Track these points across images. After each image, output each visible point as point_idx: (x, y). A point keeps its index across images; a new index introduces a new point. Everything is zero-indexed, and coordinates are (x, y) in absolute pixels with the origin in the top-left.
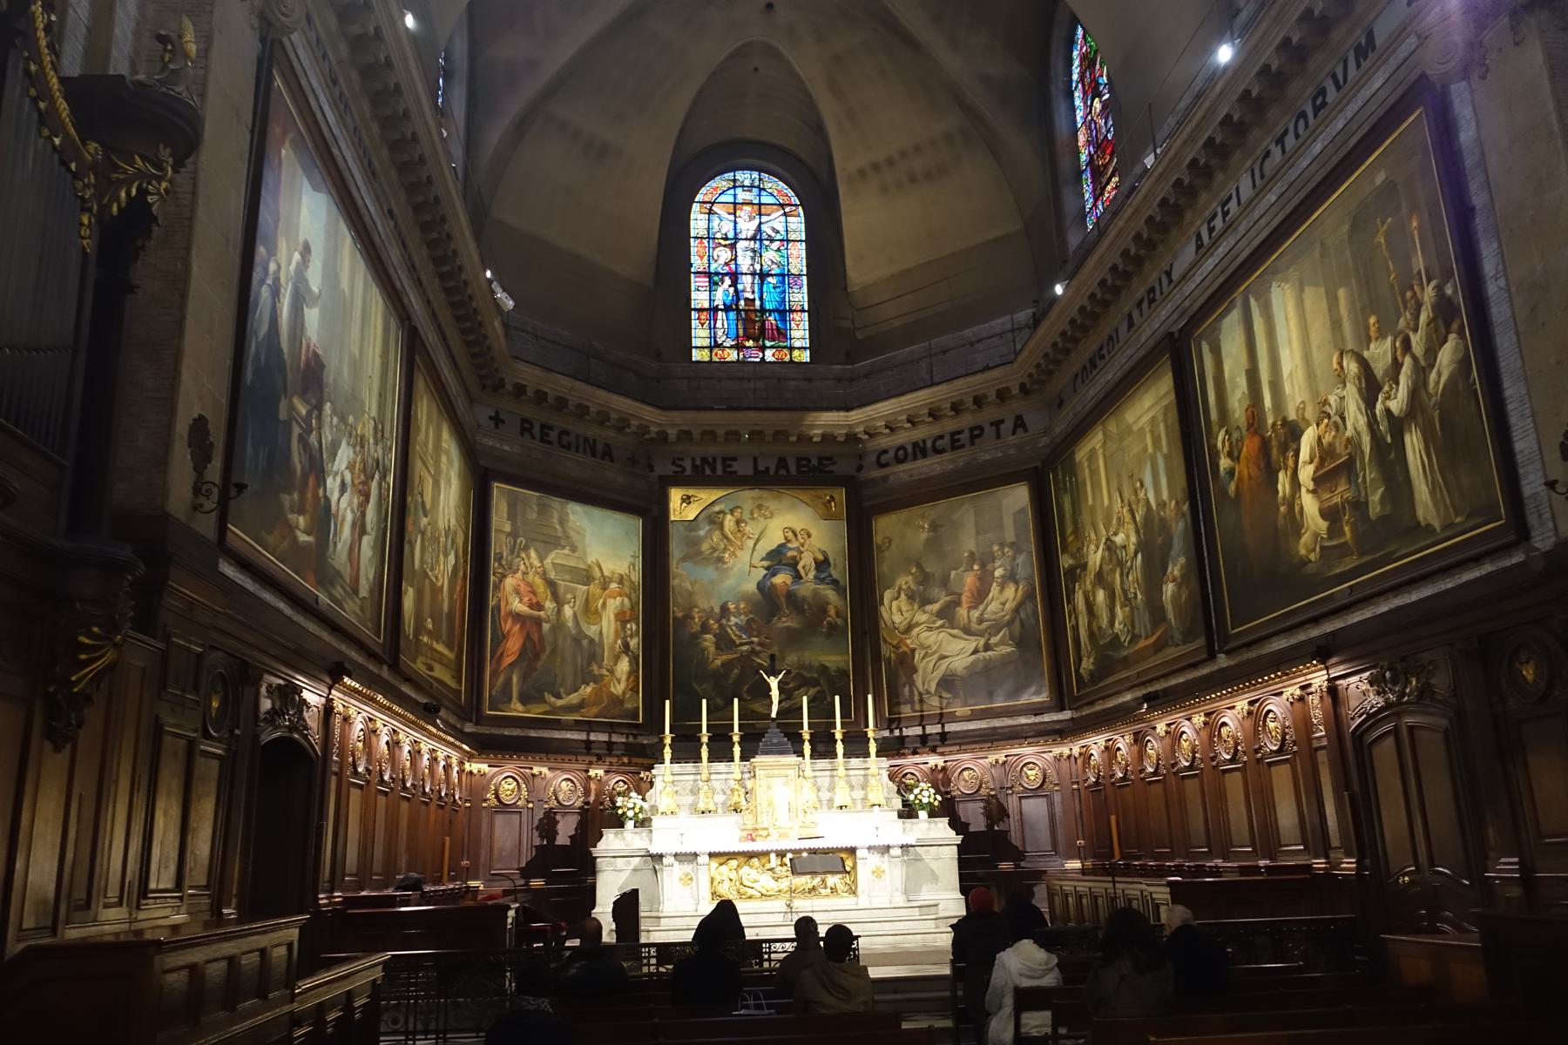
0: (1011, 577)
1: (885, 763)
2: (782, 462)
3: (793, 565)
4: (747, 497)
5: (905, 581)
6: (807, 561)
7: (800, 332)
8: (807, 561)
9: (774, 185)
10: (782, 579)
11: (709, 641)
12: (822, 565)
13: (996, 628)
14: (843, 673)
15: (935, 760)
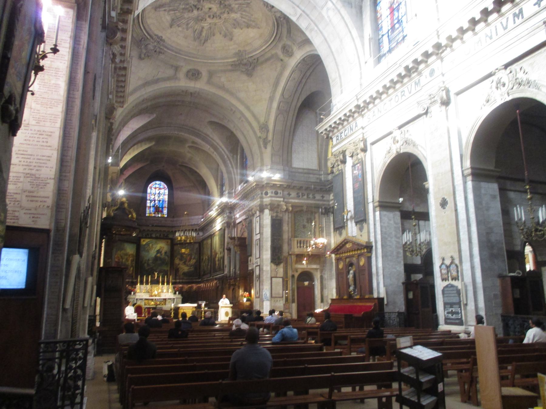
0: (194, 258)
1: (173, 286)
2: (160, 235)
3: (161, 252)
4: (154, 241)
5: (179, 257)
6: (163, 252)
7: (165, 211)
8: (163, 252)
9: (162, 183)
10: (159, 255)
11: (146, 265)
12: (166, 253)
13: (191, 266)
14: (168, 271)
15: (181, 286)
